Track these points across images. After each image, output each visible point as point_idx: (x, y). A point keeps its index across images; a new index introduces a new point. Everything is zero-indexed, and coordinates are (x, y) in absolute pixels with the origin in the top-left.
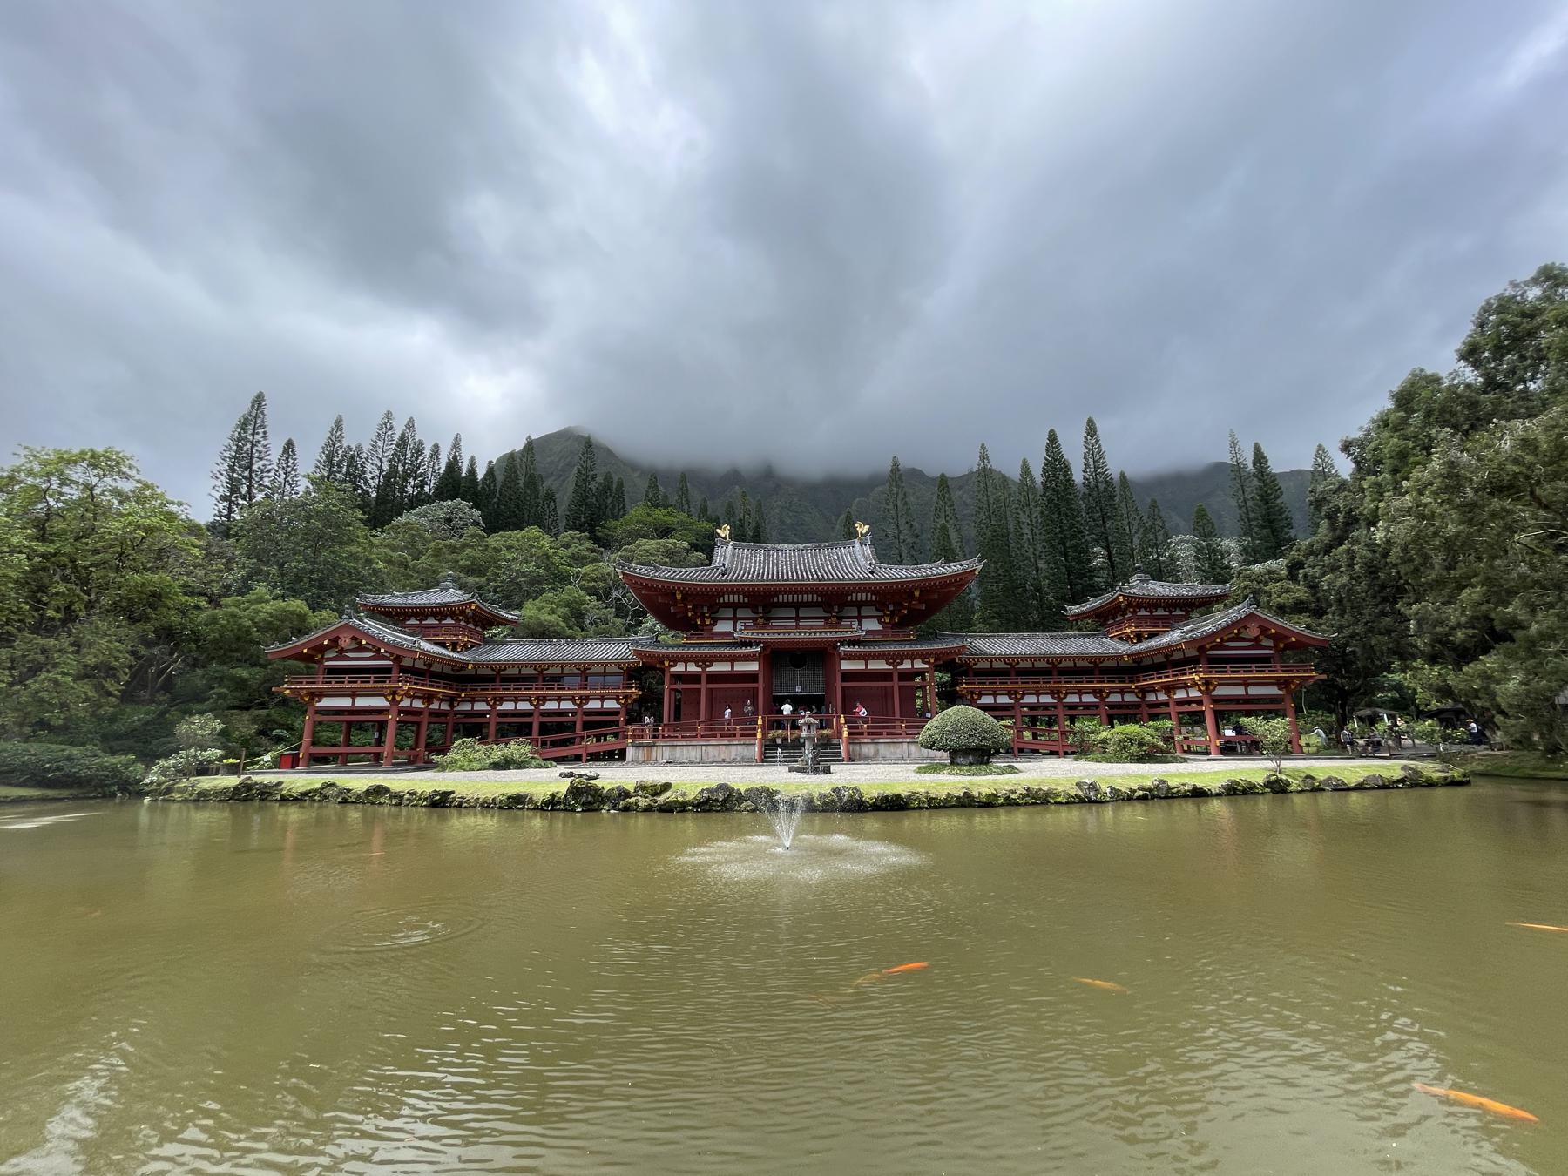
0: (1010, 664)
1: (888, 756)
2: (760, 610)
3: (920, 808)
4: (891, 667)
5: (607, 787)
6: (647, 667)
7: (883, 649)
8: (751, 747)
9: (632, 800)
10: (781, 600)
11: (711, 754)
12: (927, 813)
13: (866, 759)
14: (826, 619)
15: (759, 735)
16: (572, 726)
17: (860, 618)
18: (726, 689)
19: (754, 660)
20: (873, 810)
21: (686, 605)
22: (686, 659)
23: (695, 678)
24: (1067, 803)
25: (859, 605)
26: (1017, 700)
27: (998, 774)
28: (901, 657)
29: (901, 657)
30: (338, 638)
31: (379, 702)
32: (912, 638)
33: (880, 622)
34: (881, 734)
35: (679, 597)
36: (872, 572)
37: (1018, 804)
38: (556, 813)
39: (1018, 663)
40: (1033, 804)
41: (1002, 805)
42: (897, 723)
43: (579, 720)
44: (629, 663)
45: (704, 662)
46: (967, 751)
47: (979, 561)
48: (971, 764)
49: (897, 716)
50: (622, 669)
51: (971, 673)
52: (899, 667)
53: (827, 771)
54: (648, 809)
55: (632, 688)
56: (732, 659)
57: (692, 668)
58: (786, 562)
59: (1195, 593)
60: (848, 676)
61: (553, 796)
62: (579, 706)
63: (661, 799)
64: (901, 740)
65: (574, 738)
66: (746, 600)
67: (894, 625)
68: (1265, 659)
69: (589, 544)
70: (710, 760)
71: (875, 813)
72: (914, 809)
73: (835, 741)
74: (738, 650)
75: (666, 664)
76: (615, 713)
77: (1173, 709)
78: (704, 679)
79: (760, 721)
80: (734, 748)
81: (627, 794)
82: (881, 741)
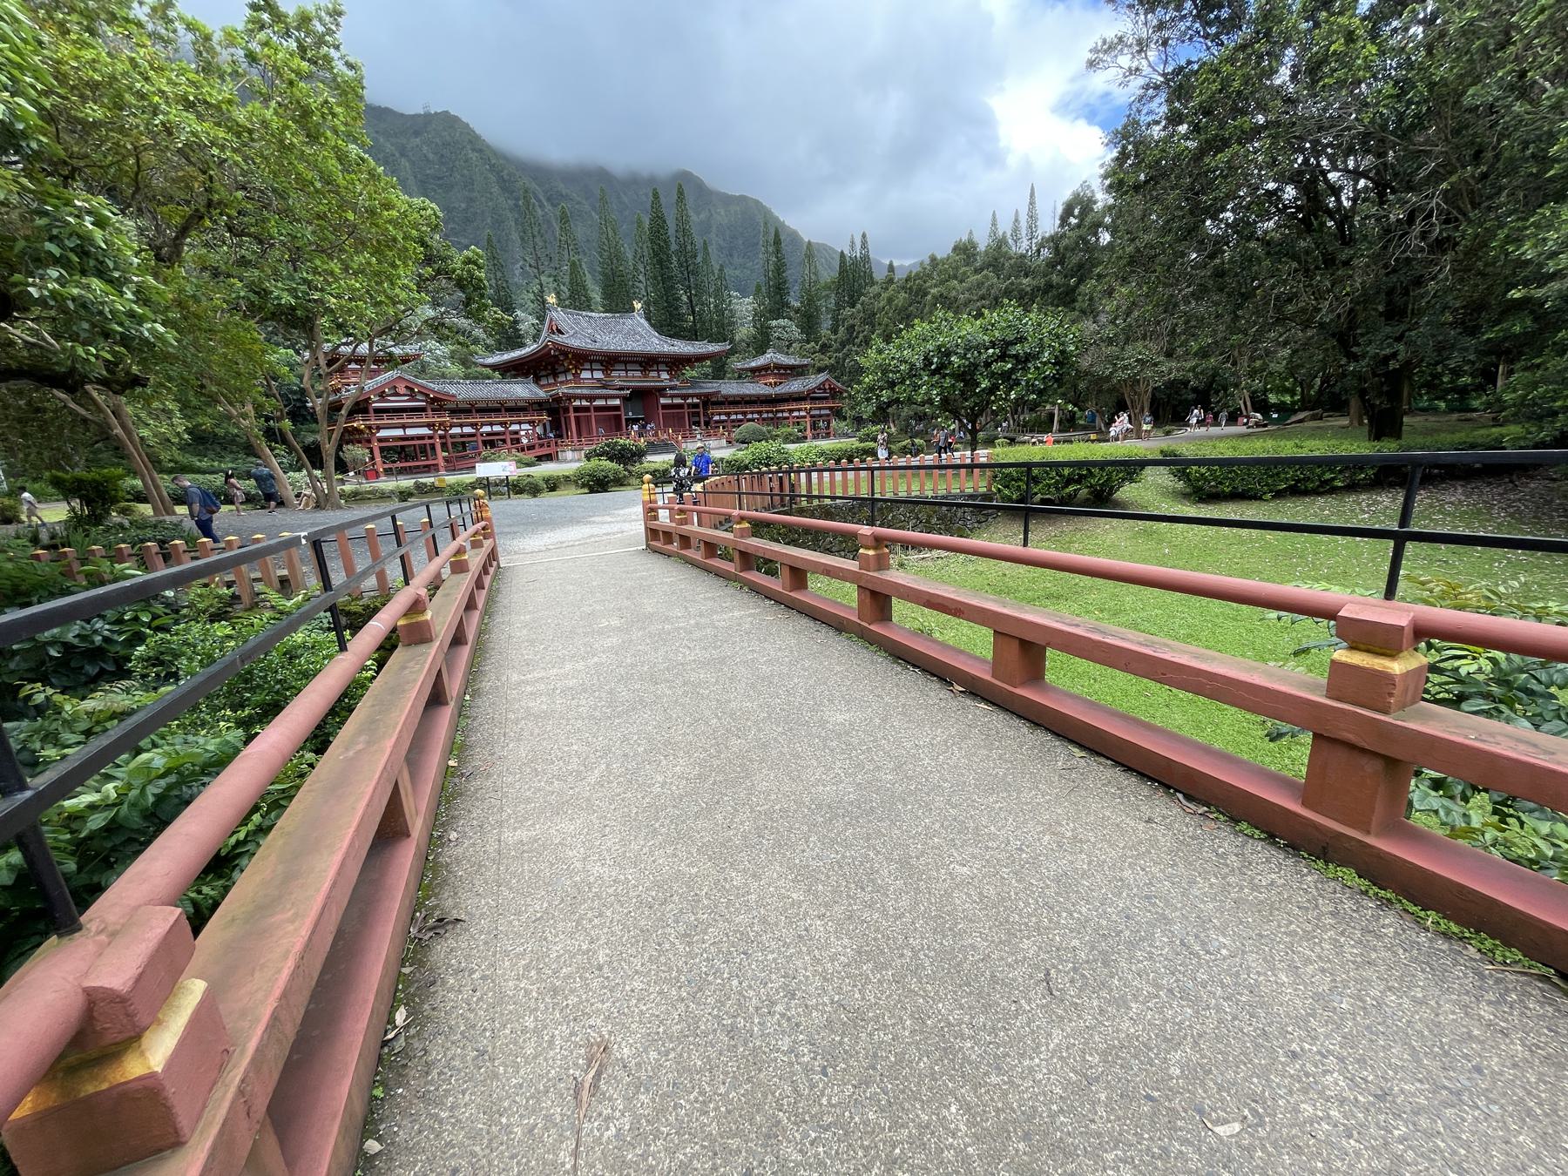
17: (658, 371)
23: (587, 409)
31: (425, 431)
56: (606, 397)
57: (585, 403)
60: (665, 407)
68: (826, 398)
77: (791, 420)
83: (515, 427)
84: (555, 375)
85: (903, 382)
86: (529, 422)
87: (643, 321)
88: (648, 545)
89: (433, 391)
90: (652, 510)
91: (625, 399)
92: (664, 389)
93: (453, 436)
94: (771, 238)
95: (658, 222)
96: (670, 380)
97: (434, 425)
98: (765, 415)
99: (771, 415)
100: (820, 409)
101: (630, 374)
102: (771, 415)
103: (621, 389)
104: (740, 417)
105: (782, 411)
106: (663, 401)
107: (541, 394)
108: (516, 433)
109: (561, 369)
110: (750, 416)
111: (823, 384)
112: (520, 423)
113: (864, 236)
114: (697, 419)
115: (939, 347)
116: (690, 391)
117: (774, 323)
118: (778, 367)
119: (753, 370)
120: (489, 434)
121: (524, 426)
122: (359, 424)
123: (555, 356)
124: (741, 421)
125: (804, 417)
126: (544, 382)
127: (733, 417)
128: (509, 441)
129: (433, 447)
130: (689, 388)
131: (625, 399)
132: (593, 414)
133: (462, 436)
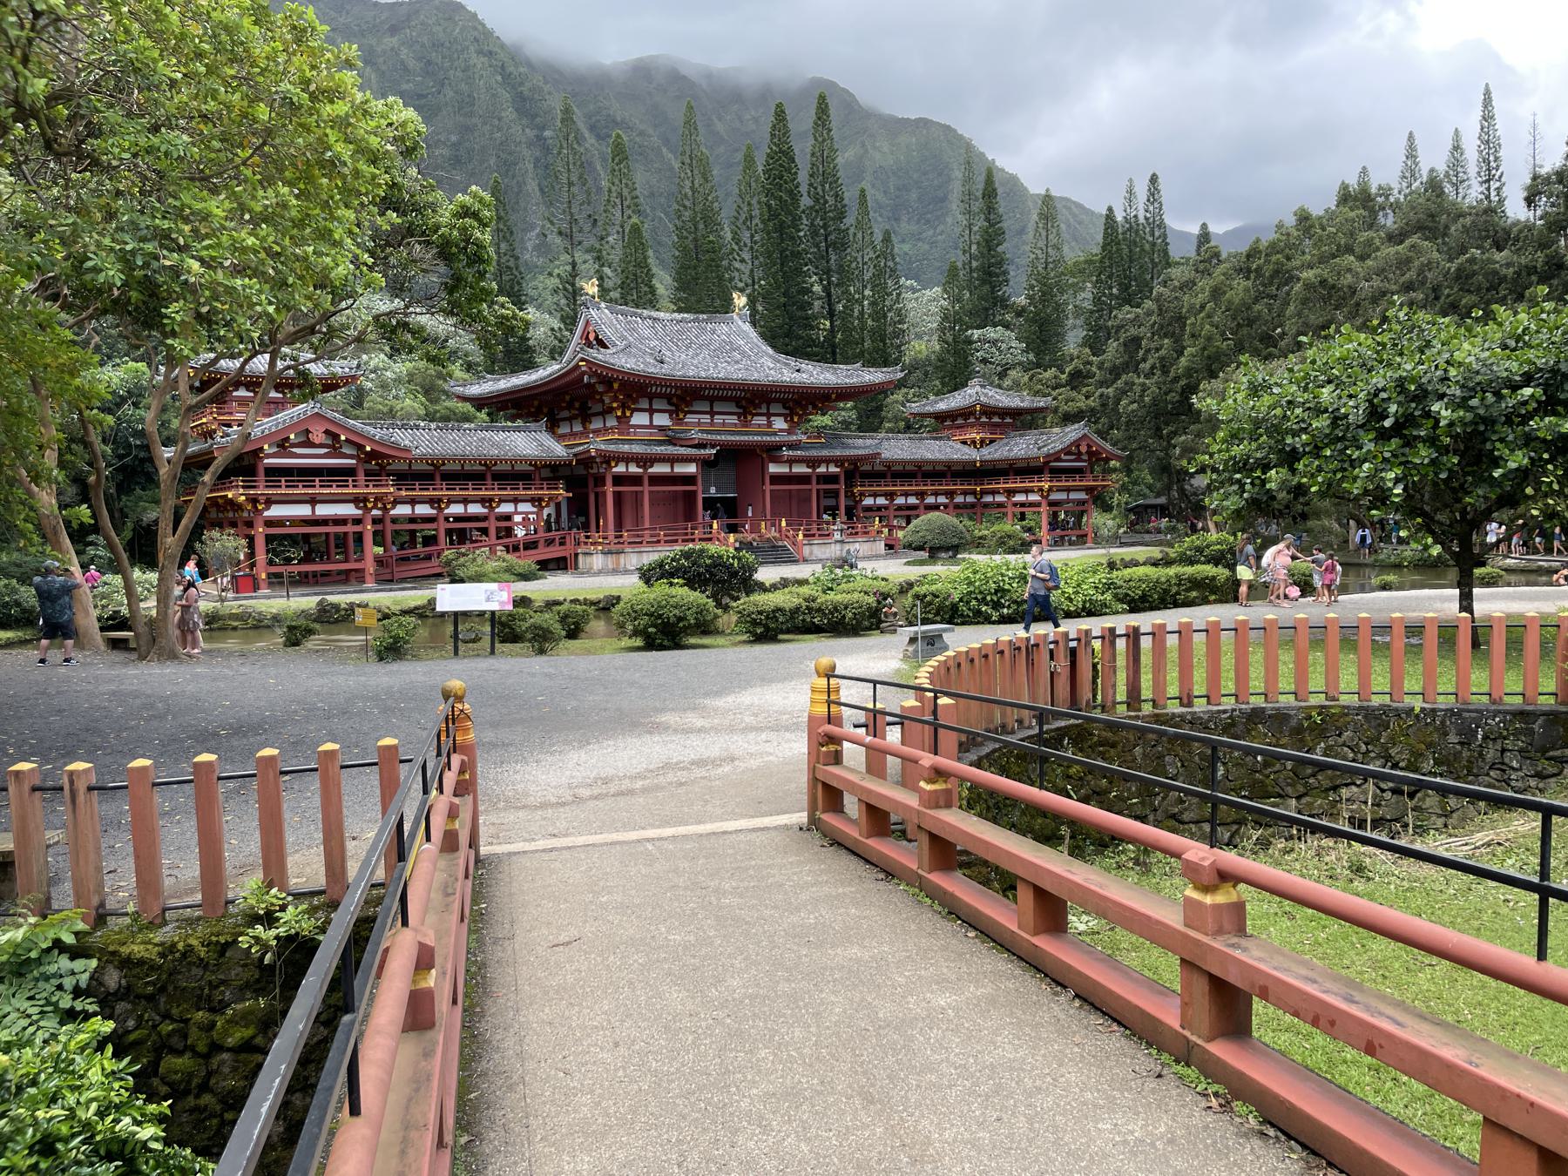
0: (889, 467)
17: (769, 415)
23: (635, 480)
30: (308, 432)
31: (348, 510)
33: (786, 421)
35: (616, 386)
36: (798, 371)
49: (815, 518)
56: (672, 460)
59: (1025, 405)
60: (777, 479)
68: (1079, 471)
83: (506, 508)
84: (586, 418)
85: (1316, 451)
86: (532, 500)
87: (747, 327)
88: (814, 823)
89: (371, 440)
90: (832, 739)
91: (705, 464)
92: (778, 447)
93: (395, 520)
94: (979, 186)
95: (782, 159)
96: (789, 432)
97: (365, 500)
98: (959, 499)
99: (970, 499)
100: (1068, 490)
101: (718, 419)
102: (970, 499)
103: (701, 445)
104: (912, 500)
105: (994, 492)
106: (773, 469)
107: (558, 450)
108: (508, 517)
109: (598, 408)
110: (930, 500)
111: (1077, 443)
112: (516, 501)
113: (1154, 179)
114: (831, 502)
115: (1401, 384)
116: (825, 453)
117: (976, 334)
118: (989, 411)
119: (941, 417)
120: (458, 519)
121: (523, 507)
122: (236, 493)
123: (589, 385)
124: (914, 507)
125: (1038, 504)
126: (564, 429)
127: (900, 501)
128: (493, 532)
129: (359, 538)
130: (823, 446)
131: (705, 464)
132: (646, 488)
133: (413, 520)
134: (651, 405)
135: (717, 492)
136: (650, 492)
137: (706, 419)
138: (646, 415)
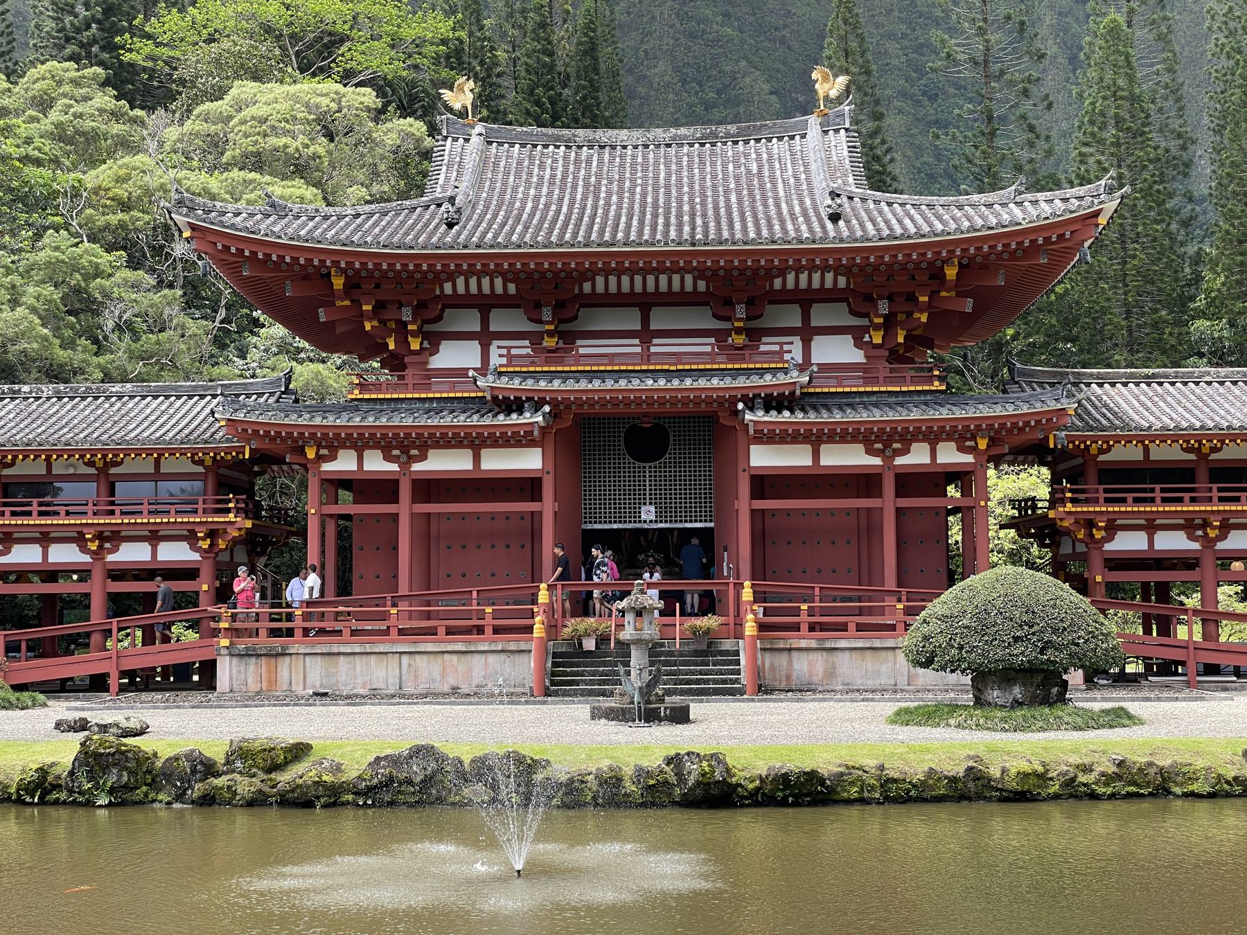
1: (859, 683)
2: (547, 314)
3: (862, 801)
4: (877, 461)
5: (165, 753)
6: (265, 459)
7: (863, 416)
8: (523, 658)
9: (220, 782)
10: (600, 288)
11: (424, 675)
12: (878, 811)
13: (802, 690)
14: (720, 335)
15: (538, 631)
16: (80, 604)
17: (807, 333)
18: (463, 516)
19: (532, 443)
20: (757, 805)
21: (357, 303)
22: (360, 442)
23: (384, 489)
24: (1212, 796)
25: (806, 300)
26: (1209, 543)
27: (1077, 728)
28: (906, 436)
29: (906, 436)
32: (937, 385)
33: (859, 344)
34: (843, 628)
35: (338, 283)
36: (835, 218)
37: (1094, 796)
38: (51, 811)
39: (1215, 450)
40: (1130, 795)
41: (1056, 797)
42: (889, 601)
43: (97, 590)
44: (217, 451)
45: (405, 450)
46: (1008, 675)
47: (1110, 190)
48: (1017, 704)
49: (890, 583)
50: (200, 463)
51: (1092, 474)
52: (900, 461)
53: (680, 716)
54: (256, 802)
55: (228, 511)
56: (476, 442)
57: (376, 463)
58: (621, 181)
60: (765, 484)
61: (43, 771)
62: (98, 555)
63: (284, 778)
64: (890, 643)
65: (88, 635)
66: (512, 288)
67: (897, 356)
69: (105, 99)
70: (421, 689)
71: (760, 811)
72: (849, 802)
73: (727, 645)
74: (487, 421)
75: (311, 453)
76: (188, 573)
78: (405, 491)
79: (543, 596)
80: (477, 660)
81: (208, 769)
82: (843, 644)
101: (660, 347)
124: (1186, 562)
130: (937, 398)
132: (405, 508)
134: (485, 322)
135: (660, 517)
136: (413, 515)
137: (632, 347)
138: (475, 346)
